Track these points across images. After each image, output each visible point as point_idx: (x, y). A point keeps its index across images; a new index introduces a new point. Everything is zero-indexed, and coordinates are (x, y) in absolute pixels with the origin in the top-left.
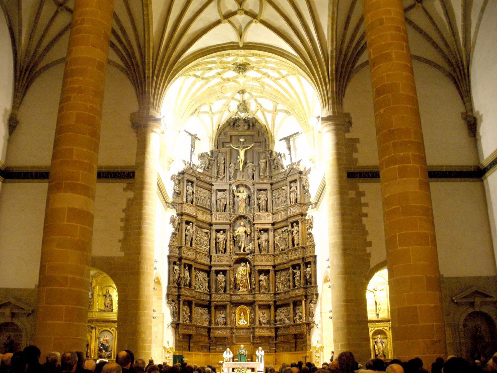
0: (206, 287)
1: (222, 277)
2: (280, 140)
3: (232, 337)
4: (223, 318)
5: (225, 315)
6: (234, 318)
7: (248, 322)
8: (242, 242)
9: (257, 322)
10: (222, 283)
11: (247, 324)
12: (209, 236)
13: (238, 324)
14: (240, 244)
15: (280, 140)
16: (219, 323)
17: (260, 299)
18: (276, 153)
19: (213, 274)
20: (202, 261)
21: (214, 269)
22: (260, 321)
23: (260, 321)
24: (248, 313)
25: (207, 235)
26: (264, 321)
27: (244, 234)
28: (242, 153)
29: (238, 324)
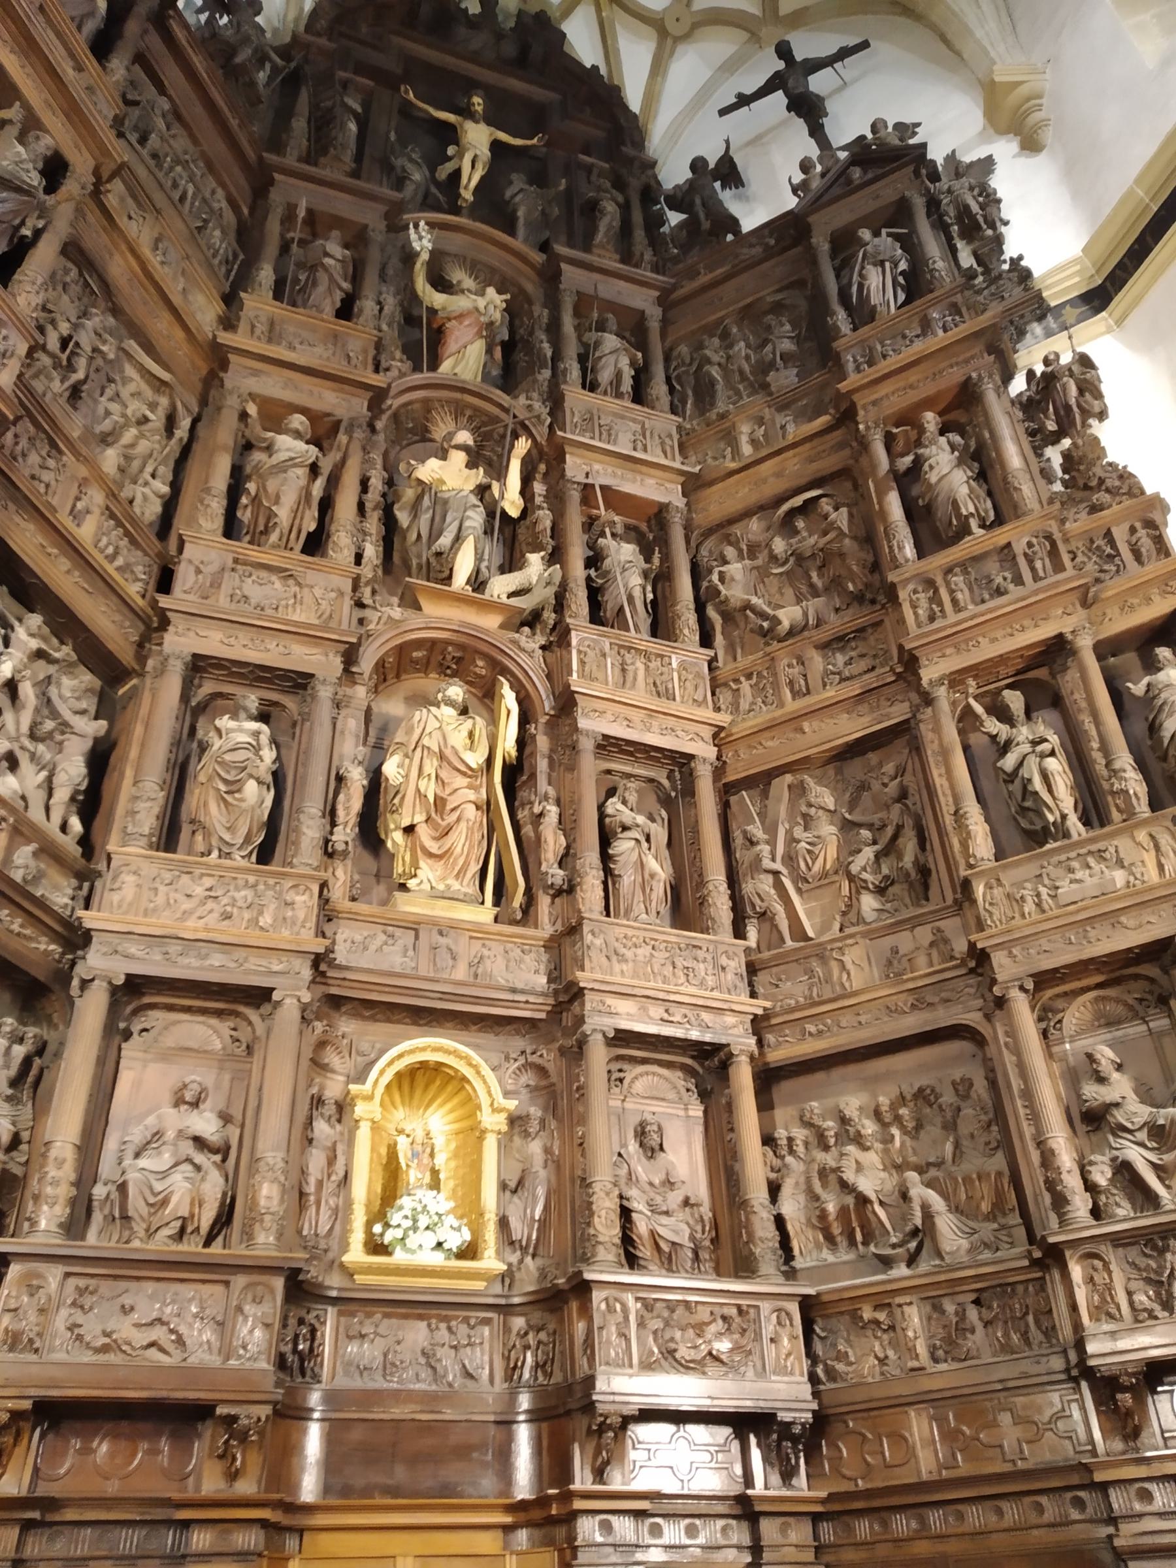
0: (62, 795)
1: (256, 734)
2: (723, 112)
3: (290, 1413)
4: (199, 1142)
5: (226, 1118)
6: (331, 1161)
7: (491, 1234)
8: (458, 539)
9: (606, 1228)
10: (251, 787)
11: (469, 1252)
12: (185, 423)
13: (376, 1247)
14: (445, 541)
15: (723, 112)
16: (137, 1204)
17: (621, 975)
18: (698, 165)
19: (160, 701)
20: (86, 532)
21: (180, 642)
22: (626, 1213)
23: (626, 1213)
24: (492, 1121)
25: (164, 401)
26: (676, 1229)
27: (474, 500)
28: (478, 137)
29: (376, 1247)
